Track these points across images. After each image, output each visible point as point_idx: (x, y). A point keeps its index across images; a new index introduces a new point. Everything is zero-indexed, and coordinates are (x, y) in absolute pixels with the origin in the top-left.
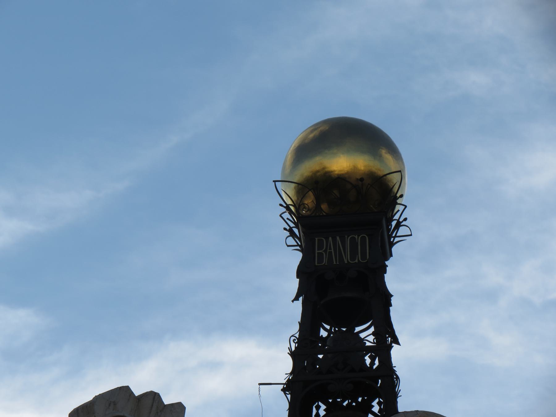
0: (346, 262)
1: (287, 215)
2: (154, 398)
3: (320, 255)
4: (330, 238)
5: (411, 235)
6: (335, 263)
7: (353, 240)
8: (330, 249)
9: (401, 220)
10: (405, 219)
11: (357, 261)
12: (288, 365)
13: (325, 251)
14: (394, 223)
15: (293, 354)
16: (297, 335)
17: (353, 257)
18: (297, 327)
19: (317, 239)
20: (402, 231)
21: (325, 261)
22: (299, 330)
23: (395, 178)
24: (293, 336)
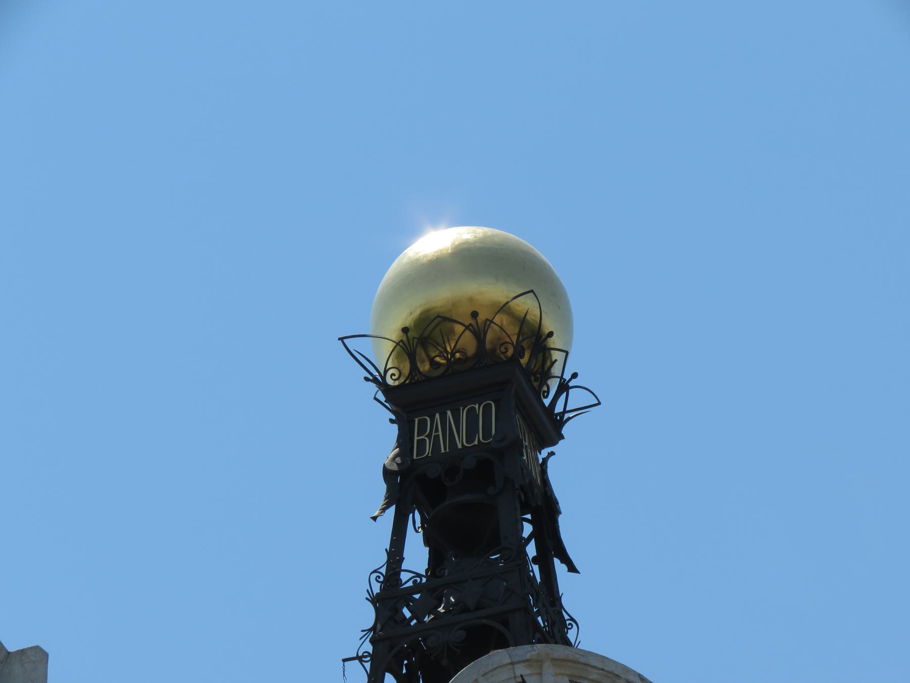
0: (460, 446)
1: (382, 398)
3: (421, 443)
4: (437, 416)
5: (599, 403)
6: (443, 451)
7: (471, 412)
8: (437, 430)
9: (567, 376)
10: (575, 376)
11: (476, 442)
12: (368, 616)
13: (429, 436)
14: (554, 385)
15: (375, 600)
16: (383, 570)
19: (416, 420)
20: (576, 398)
21: (428, 450)
22: (388, 562)
23: (526, 305)
24: (375, 571)
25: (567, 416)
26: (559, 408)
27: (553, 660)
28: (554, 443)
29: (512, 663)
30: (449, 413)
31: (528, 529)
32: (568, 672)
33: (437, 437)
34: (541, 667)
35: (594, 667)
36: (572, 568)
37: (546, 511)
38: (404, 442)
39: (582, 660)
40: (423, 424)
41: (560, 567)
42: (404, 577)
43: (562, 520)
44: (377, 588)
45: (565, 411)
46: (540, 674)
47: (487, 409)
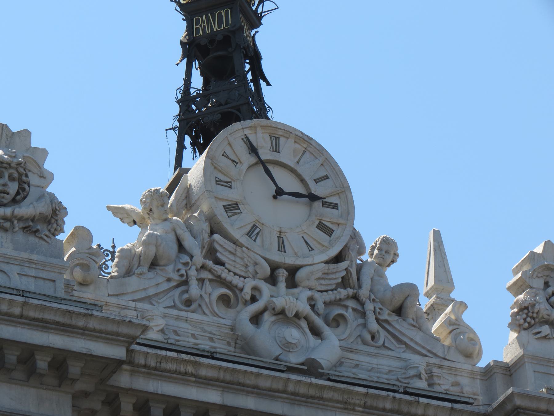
0: (215, 30)
1: (179, 9)
2: (3, 128)
3: (197, 29)
4: (204, 16)
5: (278, 8)
7: (220, 15)
8: (204, 23)
11: (222, 28)
12: (176, 109)
15: (179, 102)
16: (182, 88)
17: (219, 26)
18: (182, 83)
21: (201, 32)
22: (184, 84)
24: (179, 89)
25: (263, 14)
26: (259, 11)
27: (261, 126)
28: (258, 27)
29: (243, 129)
30: (209, 15)
31: (247, 67)
32: (269, 131)
33: (204, 26)
34: (256, 130)
35: (280, 129)
36: (268, 84)
37: (256, 58)
38: (190, 29)
39: (275, 126)
40: (198, 21)
41: (263, 84)
42: (192, 91)
43: (263, 62)
44: (180, 97)
45: (262, 12)
46: (256, 133)
47: (227, 13)
